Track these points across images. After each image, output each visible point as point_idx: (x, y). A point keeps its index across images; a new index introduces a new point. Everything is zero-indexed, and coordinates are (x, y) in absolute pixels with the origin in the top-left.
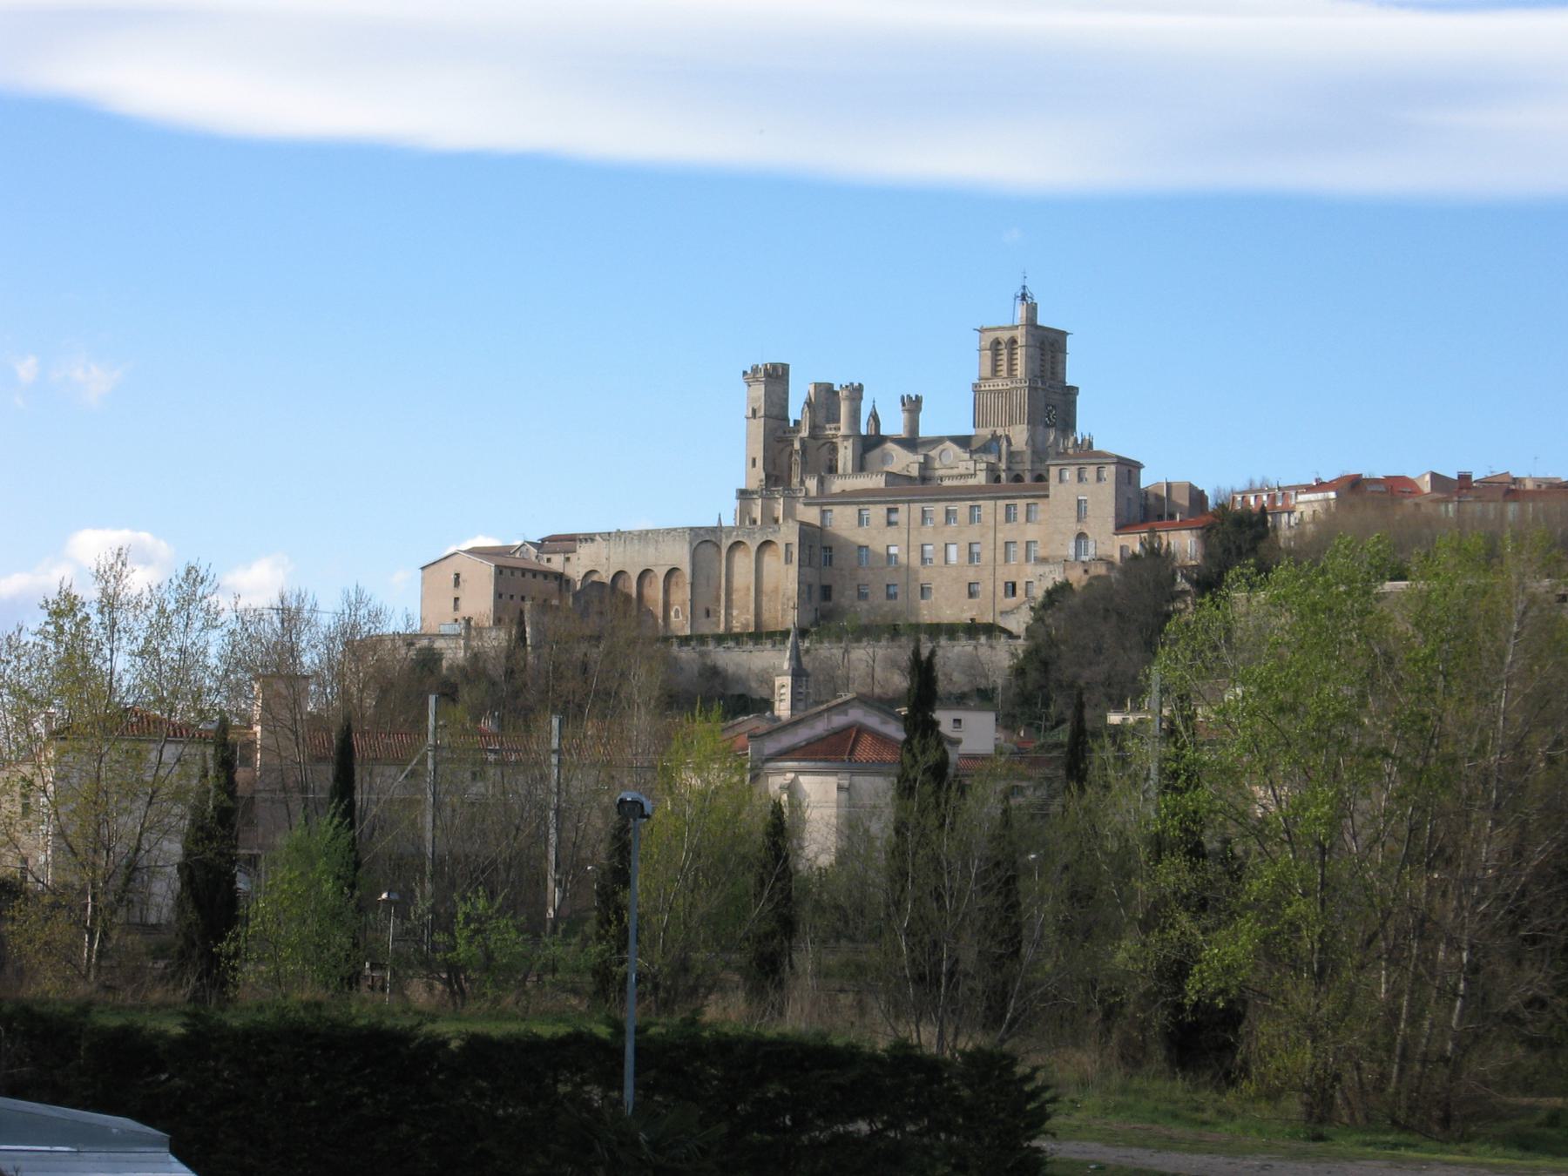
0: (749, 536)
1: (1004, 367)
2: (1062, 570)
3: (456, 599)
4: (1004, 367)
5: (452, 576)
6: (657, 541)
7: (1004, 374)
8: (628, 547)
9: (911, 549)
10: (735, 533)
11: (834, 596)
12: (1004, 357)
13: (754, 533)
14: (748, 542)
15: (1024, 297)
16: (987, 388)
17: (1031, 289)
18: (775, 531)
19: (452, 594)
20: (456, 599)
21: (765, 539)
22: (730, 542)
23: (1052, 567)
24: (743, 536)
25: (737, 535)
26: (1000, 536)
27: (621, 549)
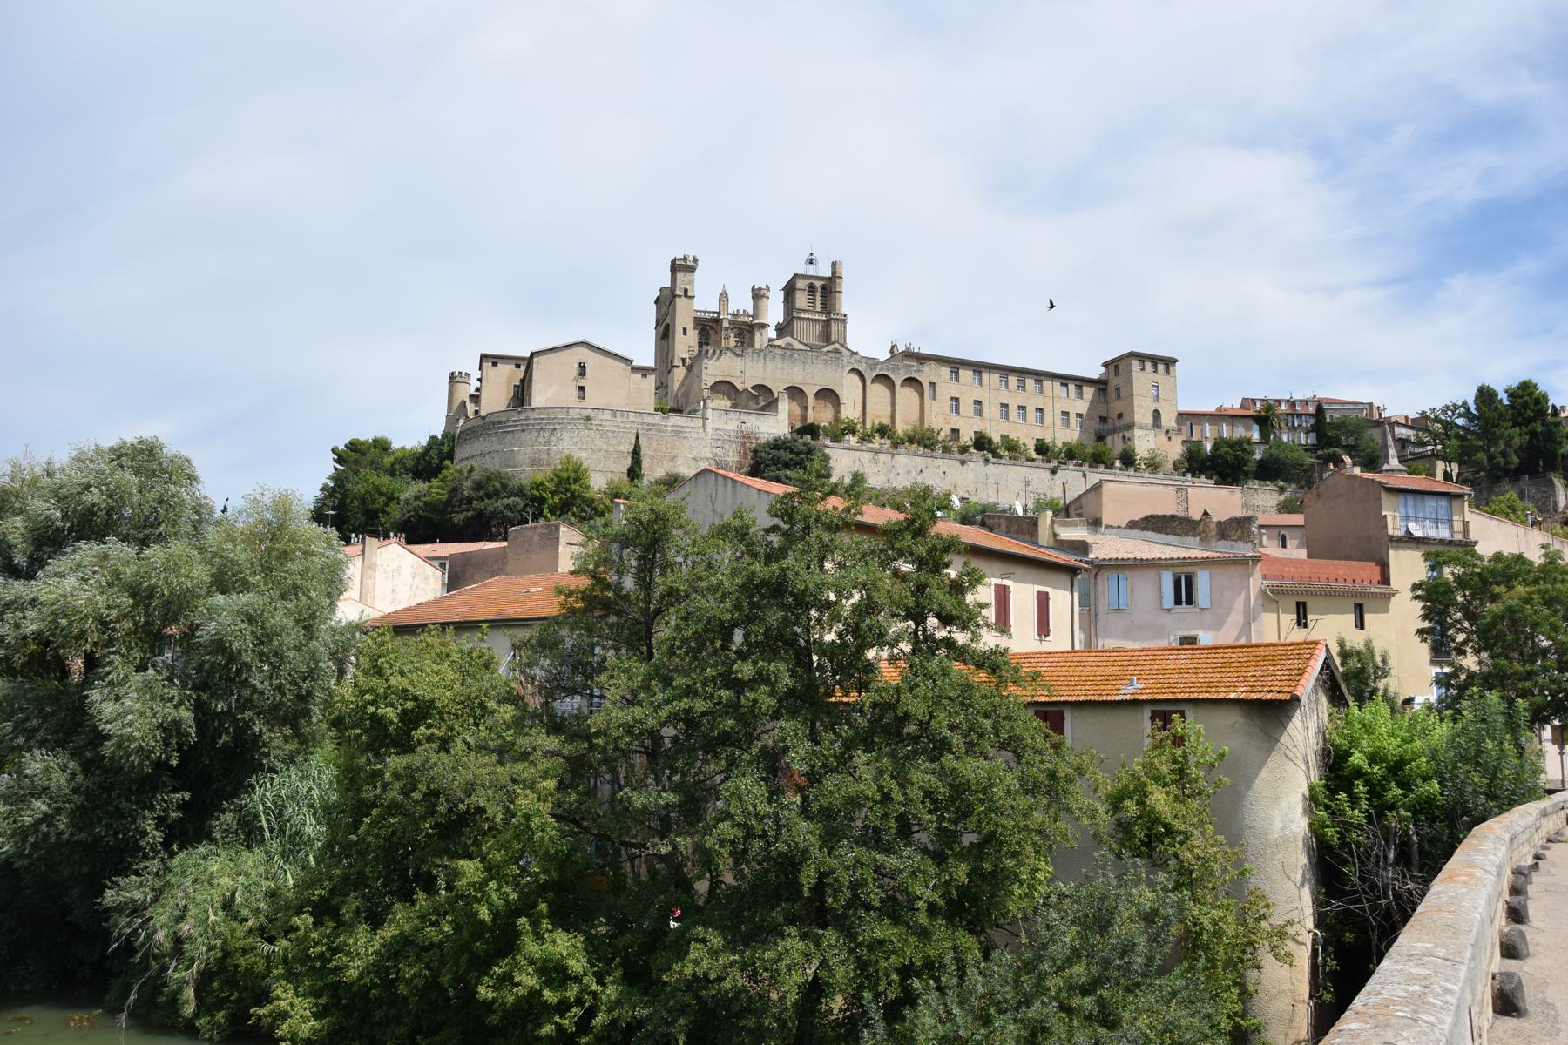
0: (893, 370)
3: (582, 389)
5: (577, 366)
7: (818, 309)
8: (769, 364)
12: (818, 297)
14: (892, 377)
16: (806, 316)
17: (816, 255)
20: (582, 389)
22: (875, 373)
23: (1147, 432)
24: (888, 370)
25: (882, 369)
26: (1057, 406)
27: (761, 364)
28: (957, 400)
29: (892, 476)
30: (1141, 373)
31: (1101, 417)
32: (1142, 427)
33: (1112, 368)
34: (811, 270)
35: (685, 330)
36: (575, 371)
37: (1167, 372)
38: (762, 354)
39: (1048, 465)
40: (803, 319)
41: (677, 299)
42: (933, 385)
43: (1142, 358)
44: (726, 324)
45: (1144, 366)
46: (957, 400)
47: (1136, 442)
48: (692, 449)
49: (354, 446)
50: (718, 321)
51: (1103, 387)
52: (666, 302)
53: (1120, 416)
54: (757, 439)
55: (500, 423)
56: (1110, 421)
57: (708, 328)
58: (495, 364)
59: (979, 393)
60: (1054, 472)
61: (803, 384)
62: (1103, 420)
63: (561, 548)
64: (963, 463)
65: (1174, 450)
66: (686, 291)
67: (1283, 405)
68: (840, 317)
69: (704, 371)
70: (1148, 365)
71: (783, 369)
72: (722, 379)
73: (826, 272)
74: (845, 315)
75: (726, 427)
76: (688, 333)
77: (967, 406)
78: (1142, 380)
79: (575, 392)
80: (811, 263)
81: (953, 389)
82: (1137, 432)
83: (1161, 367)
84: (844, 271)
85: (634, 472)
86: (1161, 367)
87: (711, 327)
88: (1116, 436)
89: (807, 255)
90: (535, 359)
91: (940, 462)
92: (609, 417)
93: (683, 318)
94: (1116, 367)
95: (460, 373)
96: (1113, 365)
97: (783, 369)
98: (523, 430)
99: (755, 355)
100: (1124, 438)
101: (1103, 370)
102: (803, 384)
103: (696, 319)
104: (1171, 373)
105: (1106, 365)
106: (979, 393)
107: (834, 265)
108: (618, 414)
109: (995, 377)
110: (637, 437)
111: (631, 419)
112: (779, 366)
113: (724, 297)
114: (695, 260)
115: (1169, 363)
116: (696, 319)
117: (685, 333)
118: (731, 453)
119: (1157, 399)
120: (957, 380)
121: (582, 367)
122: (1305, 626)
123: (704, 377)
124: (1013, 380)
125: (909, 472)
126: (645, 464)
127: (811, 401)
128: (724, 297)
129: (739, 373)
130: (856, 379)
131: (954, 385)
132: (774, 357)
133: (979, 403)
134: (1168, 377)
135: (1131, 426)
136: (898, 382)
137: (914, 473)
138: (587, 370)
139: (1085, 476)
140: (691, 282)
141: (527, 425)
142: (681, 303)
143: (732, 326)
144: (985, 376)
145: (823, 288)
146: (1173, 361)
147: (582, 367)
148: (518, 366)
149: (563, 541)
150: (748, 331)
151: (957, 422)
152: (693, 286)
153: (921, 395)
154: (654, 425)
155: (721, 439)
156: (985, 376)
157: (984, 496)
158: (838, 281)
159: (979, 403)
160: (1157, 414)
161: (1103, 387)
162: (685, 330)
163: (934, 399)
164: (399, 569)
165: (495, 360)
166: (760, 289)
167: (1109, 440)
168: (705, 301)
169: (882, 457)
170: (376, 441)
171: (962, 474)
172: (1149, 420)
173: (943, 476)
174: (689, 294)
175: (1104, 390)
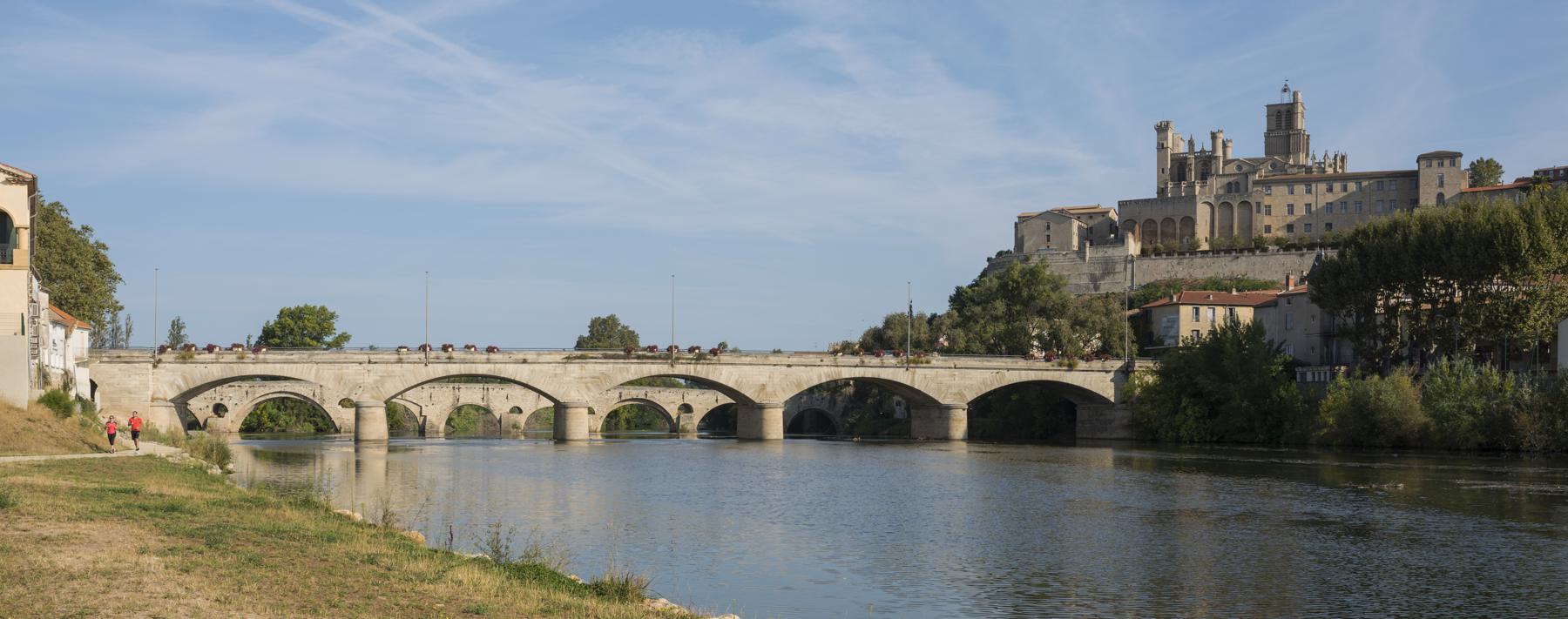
1: (1283, 124)
3: (1048, 236)
4: (1283, 124)
7: (1284, 128)
11: (1272, 231)
12: (1283, 119)
28: (1292, 205)
31: (1411, 200)
37: (1454, 165)
39: (1299, 252)
42: (1258, 204)
48: (1078, 269)
60: (1302, 255)
67: (1561, 172)
70: (1435, 163)
81: (1290, 199)
83: (1447, 162)
86: (1447, 162)
89: (1282, 86)
91: (1223, 259)
119: (1441, 184)
127: (1178, 225)
130: (1208, 208)
131: (1291, 197)
133: (1310, 205)
134: (1454, 168)
137: (1205, 267)
155: (1093, 261)
156: (1314, 186)
159: (1310, 205)
160: (1440, 196)
169: (1185, 261)
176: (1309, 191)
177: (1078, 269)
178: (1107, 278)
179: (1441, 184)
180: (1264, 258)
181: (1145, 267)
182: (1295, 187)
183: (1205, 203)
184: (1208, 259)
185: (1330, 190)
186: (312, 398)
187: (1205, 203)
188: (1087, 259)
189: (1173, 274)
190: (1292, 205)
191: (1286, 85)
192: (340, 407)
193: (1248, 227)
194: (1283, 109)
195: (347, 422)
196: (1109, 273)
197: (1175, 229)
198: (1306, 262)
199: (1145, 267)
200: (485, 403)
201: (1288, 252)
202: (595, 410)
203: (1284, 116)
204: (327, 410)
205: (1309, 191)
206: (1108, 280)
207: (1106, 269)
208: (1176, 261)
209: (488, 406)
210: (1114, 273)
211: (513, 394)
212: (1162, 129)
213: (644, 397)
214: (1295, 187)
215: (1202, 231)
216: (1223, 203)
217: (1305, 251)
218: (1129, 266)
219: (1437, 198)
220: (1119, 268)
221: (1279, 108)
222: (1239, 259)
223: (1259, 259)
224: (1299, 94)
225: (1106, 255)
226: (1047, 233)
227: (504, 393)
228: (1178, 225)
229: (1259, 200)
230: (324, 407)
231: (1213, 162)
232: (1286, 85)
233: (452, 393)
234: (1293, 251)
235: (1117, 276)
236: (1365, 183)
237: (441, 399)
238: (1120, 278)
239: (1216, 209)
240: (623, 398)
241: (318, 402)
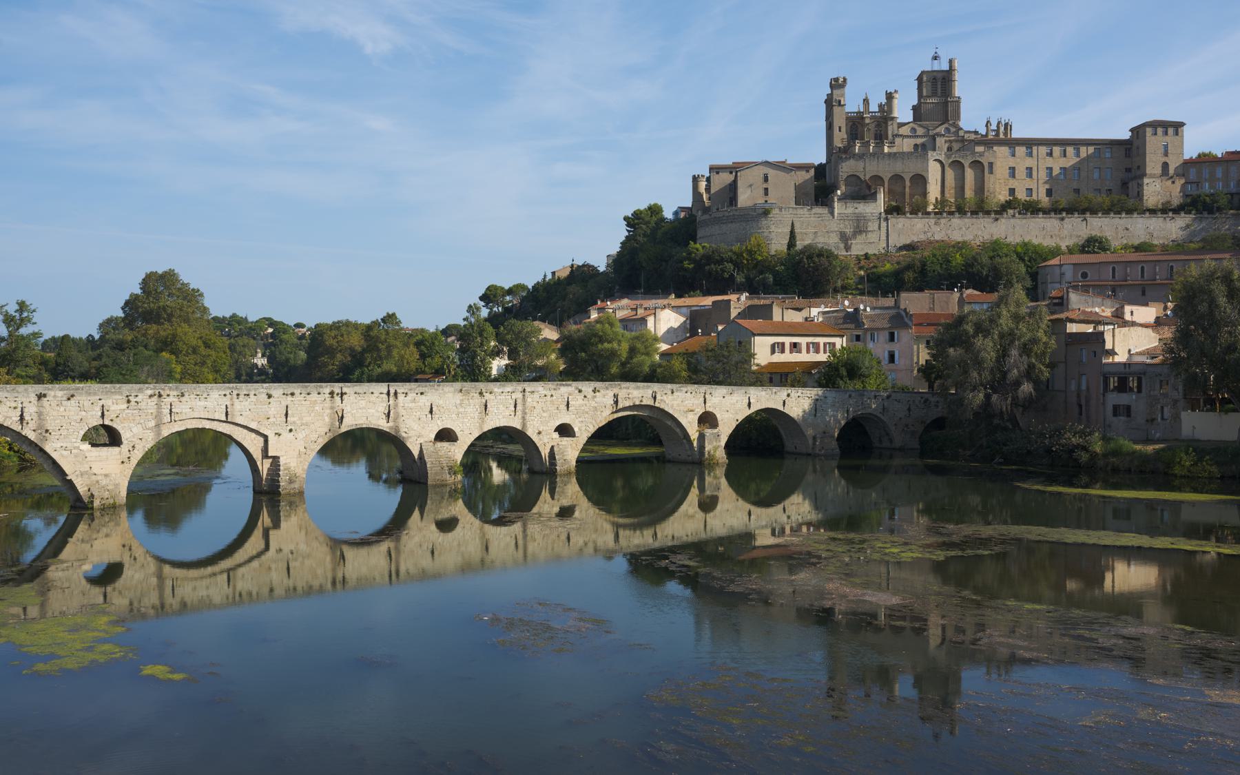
1: (939, 90)
2: (1160, 181)
3: (766, 189)
4: (939, 90)
6: (903, 159)
7: (939, 94)
9: (1039, 170)
10: (954, 156)
12: (939, 86)
13: (967, 156)
14: (963, 161)
15: (935, 58)
17: (939, 53)
18: (981, 156)
19: (770, 185)
21: (974, 159)
22: (951, 160)
23: (1154, 179)
27: (875, 162)
28: (1013, 169)
29: (949, 232)
30: (1153, 138)
31: (1126, 169)
32: (1152, 176)
33: (1135, 132)
34: (936, 66)
35: (840, 128)
36: (762, 180)
37: (1177, 134)
38: (876, 156)
39: (1059, 216)
40: (928, 103)
41: (834, 108)
42: (991, 165)
43: (1155, 125)
44: (867, 121)
45: (1156, 131)
46: (1013, 169)
47: (1145, 187)
48: (826, 226)
49: (637, 214)
50: (863, 118)
51: (1129, 146)
52: (830, 103)
53: (1139, 167)
54: (864, 217)
55: (719, 217)
56: (1133, 170)
57: (856, 124)
58: (718, 173)
59: (1030, 162)
60: (1062, 219)
61: (902, 172)
62: (1128, 170)
63: (731, 310)
64: (997, 220)
65: (1174, 191)
66: (840, 101)
68: (955, 99)
69: (841, 170)
70: (1160, 130)
71: (889, 164)
72: (852, 173)
73: (945, 67)
74: (959, 98)
75: (846, 212)
76: (842, 130)
77: (1021, 172)
78: (1154, 144)
79: (762, 192)
80: (936, 59)
82: (1146, 181)
83: (1171, 131)
84: (956, 65)
85: (791, 244)
86: (1171, 131)
87: (859, 123)
88: (1134, 182)
89: (932, 54)
90: (739, 174)
91: (982, 220)
92: (778, 212)
93: (839, 121)
94: (1138, 132)
95: (698, 175)
96: (1138, 131)
97: (889, 164)
98: (732, 222)
99: (872, 157)
100: (1138, 184)
101: (1130, 134)
102: (902, 172)
103: (849, 119)
104: (1180, 134)
105: (1132, 130)
106: (1030, 162)
107: (951, 61)
108: (783, 209)
109: (1043, 150)
110: (793, 223)
111: (790, 212)
112: (888, 162)
113: (866, 101)
114: (845, 80)
115: (1178, 126)
116: (849, 119)
117: (840, 131)
118: (849, 227)
119: (1166, 154)
120: (1014, 155)
121: (766, 179)
122: (889, 352)
123: (841, 174)
124: (1057, 150)
125: (961, 228)
126: (798, 237)
127: (908, 183)
128: (866, 101)
129: (862, 170)
130: (938, 165)
131: (1011, 159)
132: (884, 157)
133: (1031, 168)
134: (1177, 137)
135: (1144, 175)
136: (966, 165)
137: (964, 229)
138: (769, 178)
139: (1085, 219)
140: (843, 95)
141: (734, 219)
142: (836, 110)
143: (873, 121)
144: (1035, 148)
145: (944, 79)
146: (1182, 124)
147: (766, 179)
148: (731, 173)
149: (732, 307)
150: (884, 123)
151: (1013, 183)
152: (844, 98)
153: (983, 171)
154: (804, 214)
155: (843, 218)
156: (1035, 148)
157: (1012, 240)
158: (953, 73)
159: (1031, 168)
160: (1165, 166)
161: (1129, 146)
162: (840, 128)
163: (991, 172)
164: (669, 320)
165: (717, 170)
166: (891, 93)
167: (1130, 184)
168: (852, 104)
169: (943, 221)
170: (650, 208)
171: (996, 227)
172: (1159, 171)
173: (984, 229)
174: (842, 103)
175: (1130, 149)
176: (1030, 155)
177: (826, 226)
178: (859, 237)
179: (1166, 154)
180: (1024, 221)
181: (900, 226)
182: (1017, 148)
183: (935, 160)
184: (966, 220)
185: (1050, 154)
186: (17, 427)
187: (935, 160)
188: (836, 214)
189: (929, 235)
190: (1014, 168)
191: (936, 53)
192: (86, 447)
193: (980, 188)
194: (940, 76)
195: (104, 482)
196: (861, 232)
197: (905, 187)
198: (1065, 226)
199: (900, 226)
200: (391, 424)
201: (1048, 216)
202: (576, 429)
203: (939, 83)
204: (54, 455)
205: (1030, 155)
206: (860, 239)
207: (858, 227)
208: (933, 221)
209: (397, 429)
210: (866, 232)
211: (441, 402)
212: (837, 84)
213: (650, 402)
214: (1017, 148)
215: (934, 192)
216: (953, 162)
217: (1064, 214)
218: (884, 224)
219: (1162, 167)
220: (873, 226)
221: (935, 74)
222: (999, 221)
223: (1018, 221)
224: (956, 61)
225: (857, 211)
226: (765, 186)
227: (424, 401)
228: (908, 183)
229: (991, 160)
230: (48, 448)
231: (890, 123)
232: (936, 53)
233: (328, 404)
234: (1053, 215)
235: (870, 235)
236: (1084, 151)
237: (307, 419)
238: (872, 237)
239: (947, 168)
240: (620, 406)
241: (32, 436)
